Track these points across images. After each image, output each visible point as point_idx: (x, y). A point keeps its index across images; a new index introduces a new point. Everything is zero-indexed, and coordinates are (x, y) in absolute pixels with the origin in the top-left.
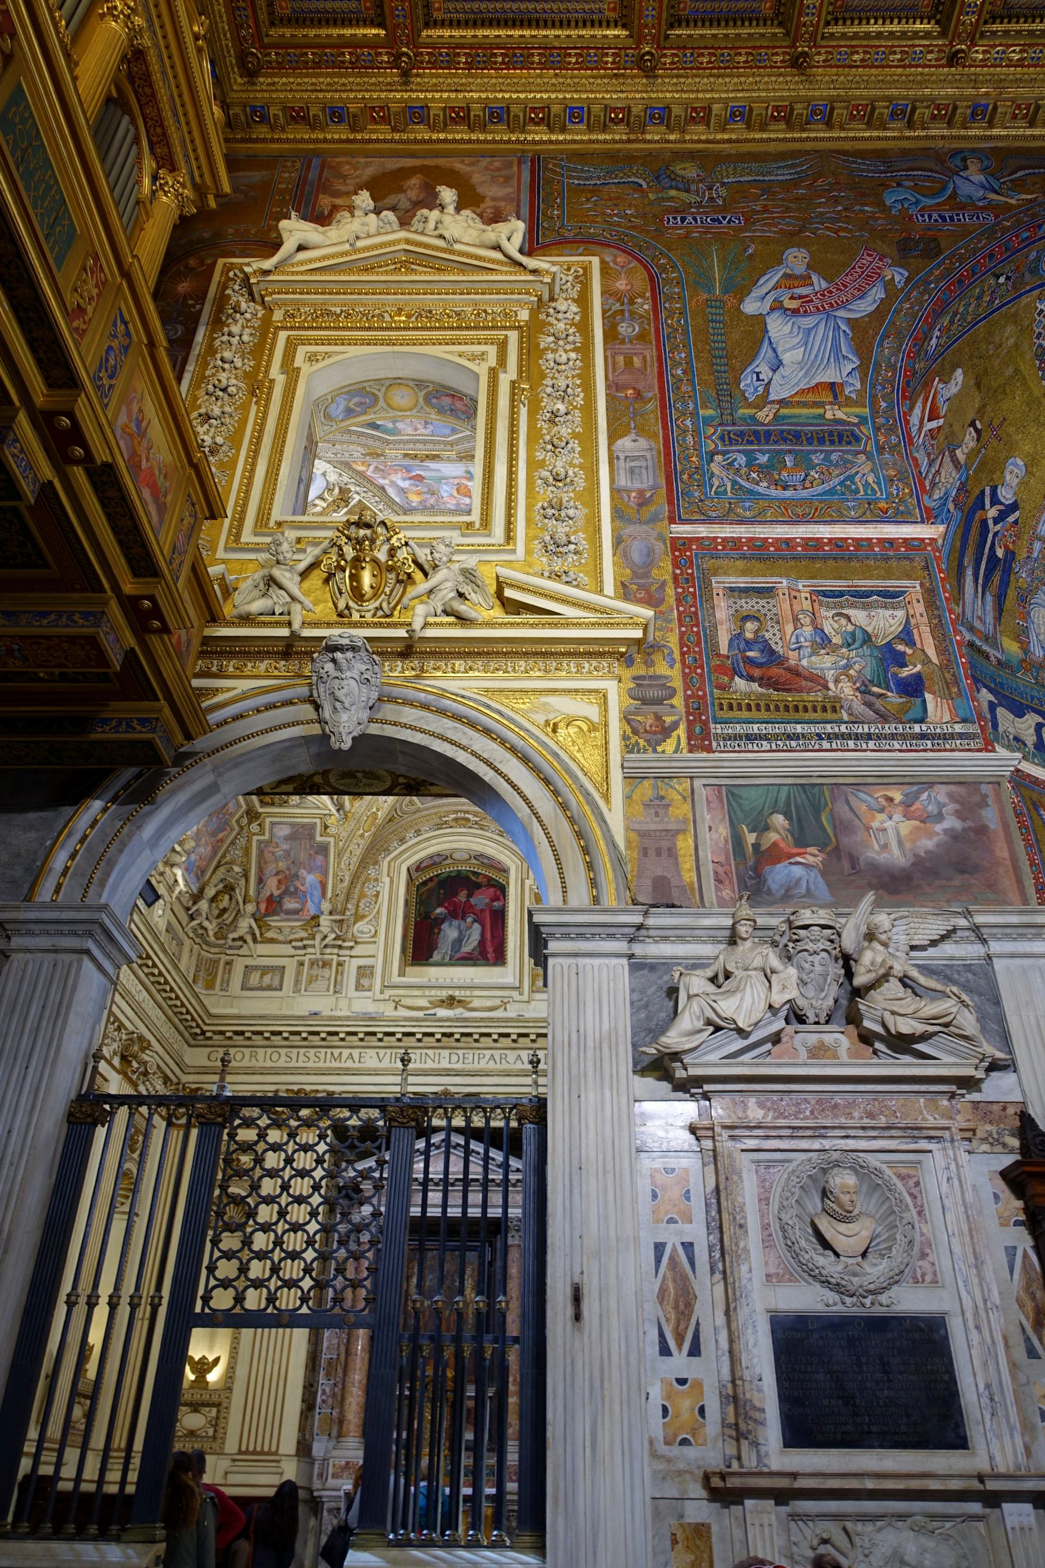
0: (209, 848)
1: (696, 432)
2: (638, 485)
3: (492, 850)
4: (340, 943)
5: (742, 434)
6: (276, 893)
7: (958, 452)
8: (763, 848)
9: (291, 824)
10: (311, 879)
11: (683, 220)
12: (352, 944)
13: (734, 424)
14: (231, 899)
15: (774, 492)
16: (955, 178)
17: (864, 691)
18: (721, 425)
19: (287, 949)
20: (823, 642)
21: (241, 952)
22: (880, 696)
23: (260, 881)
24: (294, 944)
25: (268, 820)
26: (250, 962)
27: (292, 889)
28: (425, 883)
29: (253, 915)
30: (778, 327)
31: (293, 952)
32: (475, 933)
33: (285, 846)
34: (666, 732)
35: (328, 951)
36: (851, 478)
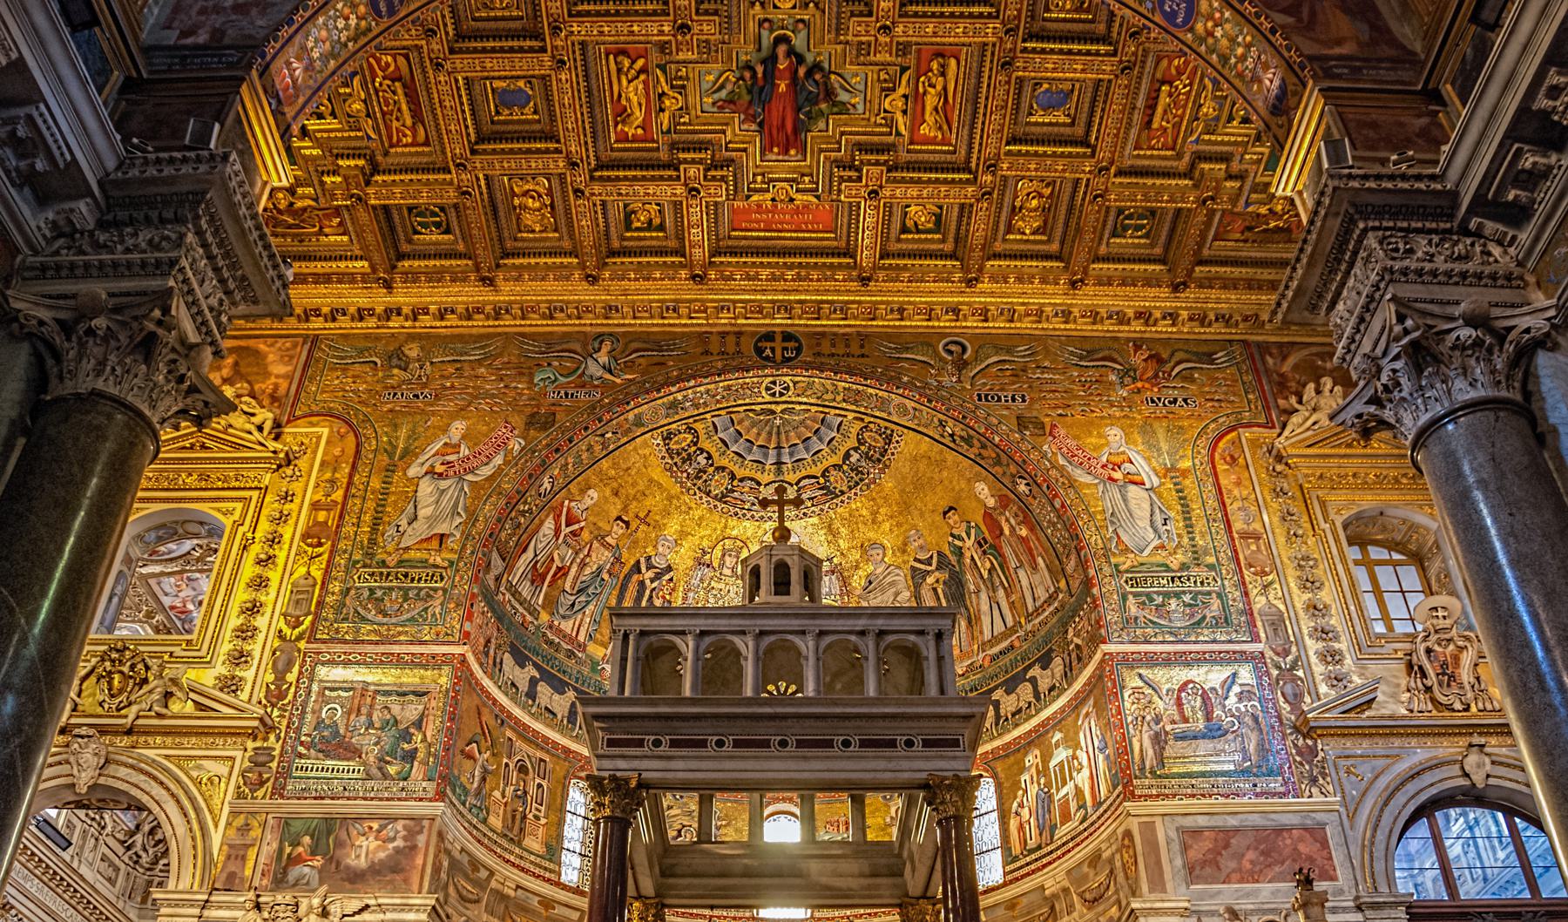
1: (347, 571)
2: (298, 613)
5: (372, 575)
7: (608, 539)
8: (295, 854)
11: (395, 394)
13: (370, 567)
15: (380, 618)
16: (589, 360)
17: (381, 760)
18: (364, 567)
20: (370, 725)
22: (388, 763)
30: (426, 488)
34: (262, 783)
36: (427, 608)
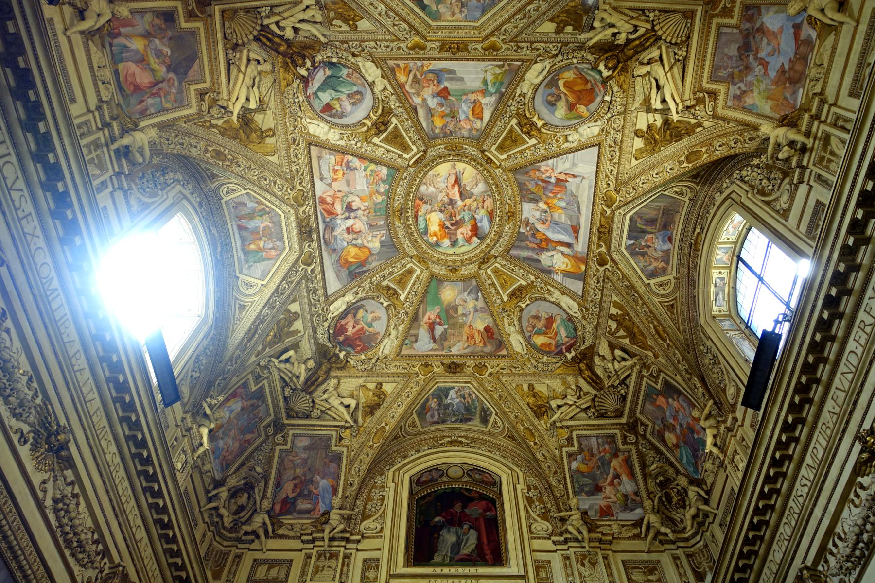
0: (237, 444)
3: (483, 462)
4: (347, 535)
6: (291, 495)
9: (311, 437)
10: (324, 483)
12: (359, 537)
14: (249, 498)
19: (298, 544)
21: (252, 546)
23: (278, 485)
24: (304, 538)
25: (291, 432)
26: (258, 555)
27: (306, 492)
28: (423, 498)
29: (268, 512)
31: (301, 546)
32: (472, 538)
33: (304, 456)
35: (336, 543)
